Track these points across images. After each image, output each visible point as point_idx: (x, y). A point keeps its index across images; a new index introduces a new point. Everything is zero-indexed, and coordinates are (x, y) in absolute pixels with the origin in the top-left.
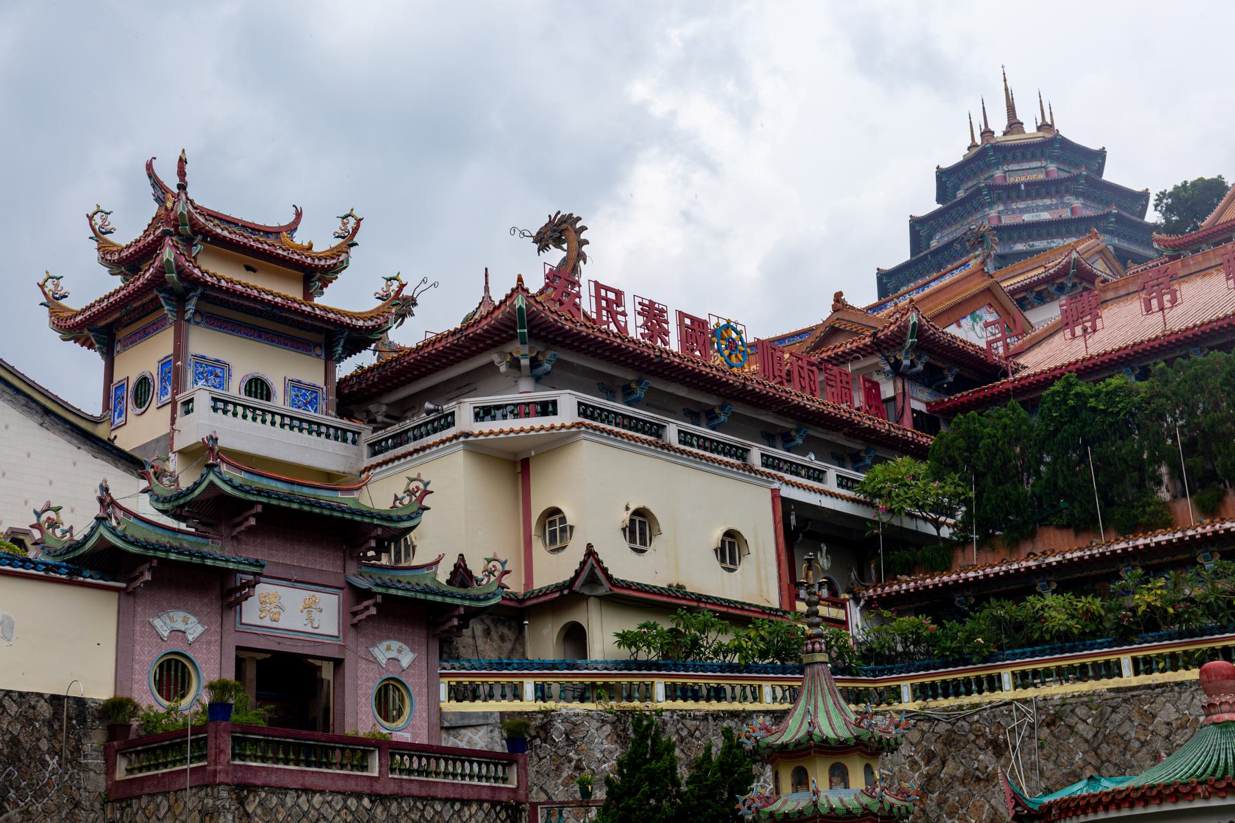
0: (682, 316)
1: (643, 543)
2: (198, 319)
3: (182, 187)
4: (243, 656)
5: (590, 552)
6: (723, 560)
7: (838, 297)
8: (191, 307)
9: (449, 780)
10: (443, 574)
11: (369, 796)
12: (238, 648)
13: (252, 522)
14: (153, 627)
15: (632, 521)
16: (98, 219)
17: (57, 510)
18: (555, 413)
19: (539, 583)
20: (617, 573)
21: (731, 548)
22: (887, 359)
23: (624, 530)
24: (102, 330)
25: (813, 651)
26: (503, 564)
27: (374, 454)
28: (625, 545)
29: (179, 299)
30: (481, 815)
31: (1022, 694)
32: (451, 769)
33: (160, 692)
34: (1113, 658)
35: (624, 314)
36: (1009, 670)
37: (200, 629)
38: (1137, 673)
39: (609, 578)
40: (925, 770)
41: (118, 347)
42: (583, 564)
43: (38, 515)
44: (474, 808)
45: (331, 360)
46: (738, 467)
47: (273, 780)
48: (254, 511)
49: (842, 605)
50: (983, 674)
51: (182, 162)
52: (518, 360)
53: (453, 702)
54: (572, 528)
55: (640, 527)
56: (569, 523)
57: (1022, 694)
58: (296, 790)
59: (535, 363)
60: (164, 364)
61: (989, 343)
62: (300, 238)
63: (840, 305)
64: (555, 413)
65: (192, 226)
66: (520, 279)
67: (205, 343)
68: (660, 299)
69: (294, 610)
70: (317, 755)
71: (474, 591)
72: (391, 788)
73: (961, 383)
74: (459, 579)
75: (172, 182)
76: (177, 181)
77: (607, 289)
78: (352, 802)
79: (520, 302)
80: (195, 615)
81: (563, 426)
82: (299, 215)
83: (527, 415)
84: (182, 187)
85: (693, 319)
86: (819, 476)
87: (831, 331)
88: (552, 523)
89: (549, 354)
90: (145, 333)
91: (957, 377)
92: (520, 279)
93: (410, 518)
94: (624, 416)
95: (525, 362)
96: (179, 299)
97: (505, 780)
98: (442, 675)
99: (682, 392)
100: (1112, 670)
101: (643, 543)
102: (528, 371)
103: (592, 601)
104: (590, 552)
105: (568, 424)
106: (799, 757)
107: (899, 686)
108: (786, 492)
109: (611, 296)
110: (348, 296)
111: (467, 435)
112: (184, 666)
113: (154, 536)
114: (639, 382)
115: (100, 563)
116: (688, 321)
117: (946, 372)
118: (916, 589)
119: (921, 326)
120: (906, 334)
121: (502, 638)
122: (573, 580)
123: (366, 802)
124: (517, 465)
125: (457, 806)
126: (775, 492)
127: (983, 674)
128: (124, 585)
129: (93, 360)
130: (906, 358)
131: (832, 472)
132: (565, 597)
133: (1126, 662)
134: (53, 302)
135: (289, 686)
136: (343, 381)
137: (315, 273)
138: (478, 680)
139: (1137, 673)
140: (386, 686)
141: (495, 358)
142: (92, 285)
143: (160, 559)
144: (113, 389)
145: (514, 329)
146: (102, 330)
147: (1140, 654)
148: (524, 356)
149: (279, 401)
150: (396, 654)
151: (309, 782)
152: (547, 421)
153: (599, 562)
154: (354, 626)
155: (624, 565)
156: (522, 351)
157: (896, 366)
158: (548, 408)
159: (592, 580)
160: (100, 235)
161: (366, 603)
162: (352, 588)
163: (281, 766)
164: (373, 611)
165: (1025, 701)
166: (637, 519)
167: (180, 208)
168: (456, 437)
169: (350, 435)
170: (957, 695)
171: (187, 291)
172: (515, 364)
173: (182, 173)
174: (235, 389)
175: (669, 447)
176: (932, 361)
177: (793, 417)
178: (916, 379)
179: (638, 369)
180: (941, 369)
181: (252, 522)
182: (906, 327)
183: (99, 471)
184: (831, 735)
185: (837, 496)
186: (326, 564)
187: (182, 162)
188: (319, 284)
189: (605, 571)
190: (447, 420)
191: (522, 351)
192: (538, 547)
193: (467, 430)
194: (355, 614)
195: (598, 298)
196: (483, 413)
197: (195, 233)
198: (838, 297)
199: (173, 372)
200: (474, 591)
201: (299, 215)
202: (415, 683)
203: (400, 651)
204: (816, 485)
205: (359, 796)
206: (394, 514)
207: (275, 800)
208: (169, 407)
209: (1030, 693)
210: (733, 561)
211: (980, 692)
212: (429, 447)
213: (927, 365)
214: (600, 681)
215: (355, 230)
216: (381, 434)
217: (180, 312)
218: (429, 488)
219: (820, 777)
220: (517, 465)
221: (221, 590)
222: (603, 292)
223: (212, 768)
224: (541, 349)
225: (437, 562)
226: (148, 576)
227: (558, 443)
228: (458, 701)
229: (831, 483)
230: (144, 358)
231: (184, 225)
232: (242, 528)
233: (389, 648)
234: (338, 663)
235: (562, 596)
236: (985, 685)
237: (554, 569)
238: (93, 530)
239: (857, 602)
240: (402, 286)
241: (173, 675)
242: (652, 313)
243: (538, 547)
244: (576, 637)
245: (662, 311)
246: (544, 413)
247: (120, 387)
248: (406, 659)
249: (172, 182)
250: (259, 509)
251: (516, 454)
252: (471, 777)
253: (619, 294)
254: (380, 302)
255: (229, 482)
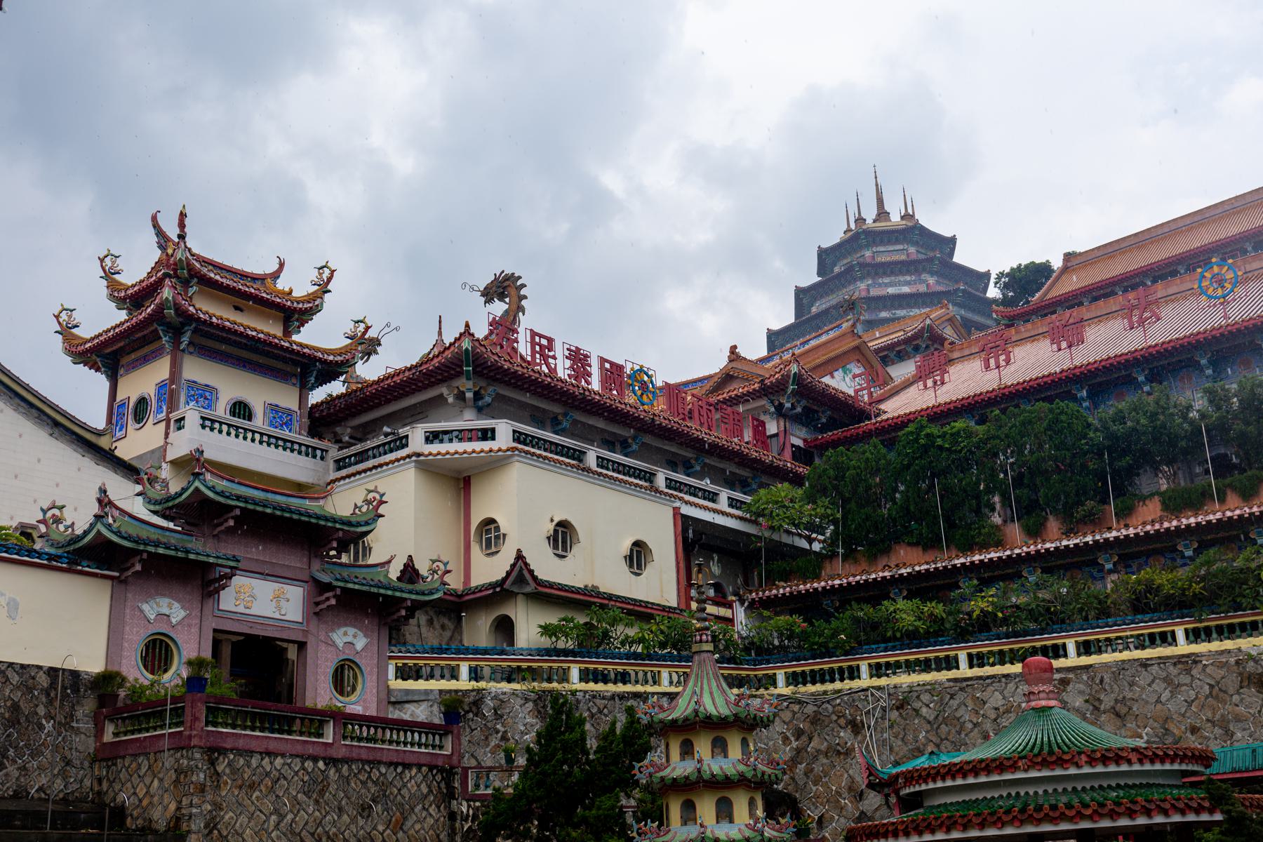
0: (603, 360)
1: (565, 549)
2: (191, 350)
3: (182, 237)
4: (219, 638)
5: (520, 557)
6: (631, 566)
7: (733, 349)
8: (185, 339)
9: (393, 747)
10: (394, 572)
11: (324, 759)
12: (215, 631)
13: (231, 523)
14: (142, 611)
15: (556, 531)
16: (108, 262)
17: (61, 508)
18: (493, 439)
19: (475, 582)
20: (541, 574)
21: (638, 556)
22: (772, 402)
23: (549, 538)
24: (109, 355)
25: (701, 641)
26: (445, 564)
27: (339, 469)
28: (549, 551)
29: (176, 332)
30: (420, 777)
31: (877, 682)
32: (395, 737)
33: (146, 667)
34: (952, 653)
35: (554, 357)
36: (866, 662)
37: (182, 614)
38: (971, 667)
39: (535, 578)
40: (795, 744)
41: (122, 371)
42: (513, 566)
43: (44, 512)
44: (414, 771)
45: (305, 388)
46: (573, 466)
47: (241, 743)
48: (233, 514)
49: (729, 605)
50: (845, 665)
51: (183, 216)
52: (463, 393)
53: (399, 681)
54: (504, 535)
55: (563, 536)
56: (502, 531)
57: (877, 682)
58: (261, 753)
59: (478, 396)
60: (161, 386)
61: (856, 391)
62: (282, 284)
64: (493, 439)
65: (189, 271)
66: (467, 325)
67: (197, 370)
68: (585, 347)
69: (264, 598)
70: (283, 724)
71: (420, 586)
72: (341, 753)
73: (832, 424)
74: (407, 576)
75: (173, 233)
76: (178, 231)
77: (541, 336)
78: (309, 765)
79: (466, 344)
80: (178, 601)
81: (500, 450)
82: (282, 265)
83: (470, 440)
84: (182, 237)
85: (612, 363)
86: (713, 497)
87: (727, 377)
88: (488, 531)
89: (491, 389)
90: (146, 360)
92: (467, 325)
93: (367, 523)
94: (551, 443)
95: (469, 395)
96: (176, 332)
97: (441, 747)
98: (391, 658)
99: (601, 424)
100: (951, 663)
101: (565, 549)
102: (471, 403)
103: (520, 598)
104: (520, 557)
105: (504, 448)
106: (688, 729)
108: (687, 510)
109: (544, 342)
110: (322, 334)
111: (419, 455)
112: (167, 645)
113: (145, 533)
114: (565, 415)
115: (100, 556)
116: (607, 366)
118: (791, 593)
121: (443, 627)
122: (504, 580)
123: (321, 764)
124: (460, 482)
125: (399, 769)
126: (676, 510)
127: (845, 665)
128: (117, 574)
129: (100, 382)
131: (724, 495)
132: (499, 593)
133: (963, 657)
134: (66, 331)
135: (259, 666)
136: (314, 407)
137: (295, 314)
138: (421, 662)
139: (971, 667)
140: (342, 666)
141: (444, 390)
142: (101, 317)
143: (149, 553)
144: (115, 406)
145: (461, 367)
146: (109, 355)
147: (974, 651)
148: (469, 390)
149: (259, 422)
150: (351, 639)
151: (272, 746)
152: (486, 445)
153: (526, 564)
154: (315, 613)
155: (547, 567)
156: (467, 385)
157: (781, 405)
158: (488, 434)
159: (520, 580)
160: (109, 275)
161: (327, 595)
162: (316, 582)
163: (248, 732)
164: (333, 602)
165: (879, 688)
166: (560, 529)
167: (179, 255)
168: (409, 456)
169: (319, 453)
170: (823, 682)
171: (183, 325)
172: (461, 396)
173: (182, 225)
174: (221, 410)
175: (588, 470)
177: (693, 448)
179: (565, 404)
180: (817, 412)
181: (231, 523)
182: (788, 376)
183: (98, 475)
184: (714, 712)
185: (727, 515)
186: (294, 560)
187: (183, 216)
188: (297, 324)
189: (531, 572)
190: (402, 442)
191: (467, 385)
192: (476, 551)
193: (418, 450)
194: (317, 604)
195: (533, 344)
196: (432, 437)
197: (192, 277)
198: (733, 349)
199: (169, 394)
200: (420, 586)
201: (282, 265)
202: (368, 664)
203: (355, 636)
204: (710, 505)
205: (315, 759)
206: (353, 520)
207: (242, 761)
208: (164, 424)
209: (883, 681)
210: (639, 567)
211: (842, 680)
212: (387, 464)
213: (804, 408)
214: (524, 665)
215: (330, 279)
216: (346, 452)
217: (176, 342)
218: (384, 499)
219: (703, 747)
220: (460, 482)
221: (202, 580)
222: (537, 339)
223: (187, 733)
224: (483, 384)
225: (389, 562)
226: (138, 567)
227: (495, 464)
228: (404, 679)
229: (723, 504)
230: (144, 381)
231: (183, 270)
232: (222, 528)
233: (345, 634)
234: (302, 646)
235: (495, 593)
236: (846, 675)
237: (489, 569)
238: (92, 526)
239: (742, 604)
240: (368, 328)
241: (158, 652)
242: (578, 358)
243: (476, 551)
244: (505, 627)
245: (586, 356)
246: (484, 438)
247: (122, 405)
248: (360, 643)
249: (173, 233)
250: (238, 512)
251: (459, 472)
252: (412, 744)
253: (550, 340)
254: (349, 341)
255: (212, 489)
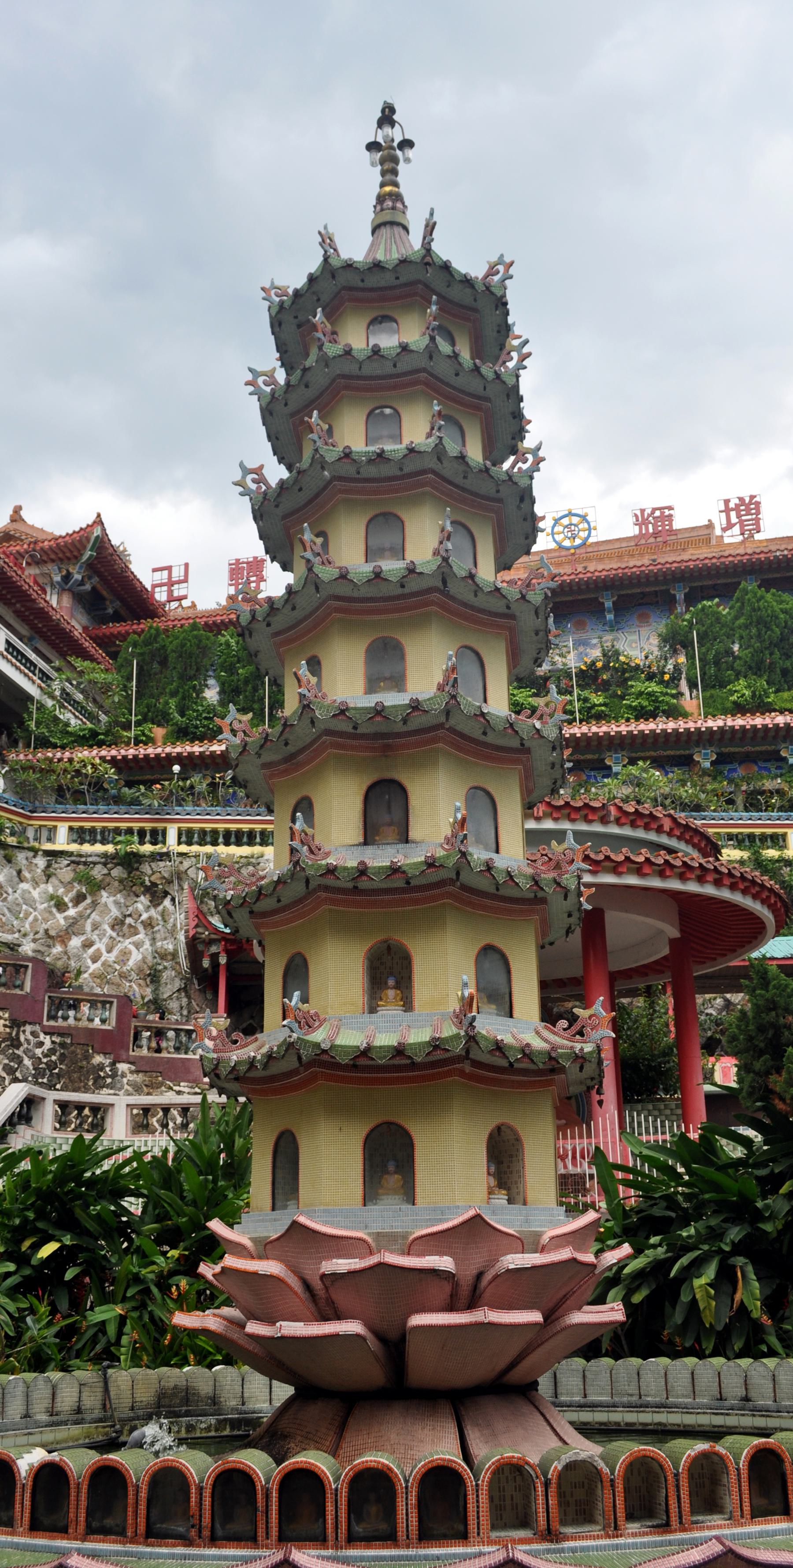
22: (60, 569)
40: (72, 912)
61: (154, 586)
63: (17, 517)
73: (117, 618)
91: (116, 612)
107: (55, 827)
117: (108, 603)
119: (102, 541)
120: (85, 548)
130: (79, 573)
176: (99, 586)
178: (79, 598)
182: (88, 539)
198: (17, 510)
236: (148, 838)
